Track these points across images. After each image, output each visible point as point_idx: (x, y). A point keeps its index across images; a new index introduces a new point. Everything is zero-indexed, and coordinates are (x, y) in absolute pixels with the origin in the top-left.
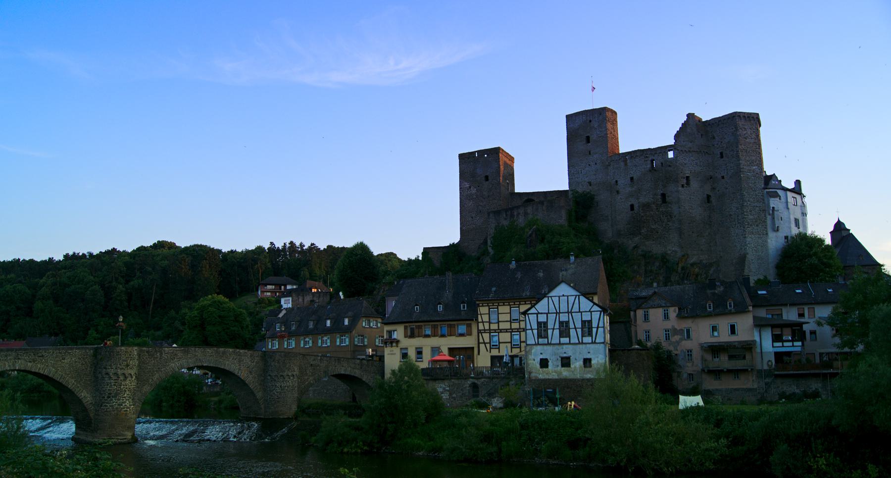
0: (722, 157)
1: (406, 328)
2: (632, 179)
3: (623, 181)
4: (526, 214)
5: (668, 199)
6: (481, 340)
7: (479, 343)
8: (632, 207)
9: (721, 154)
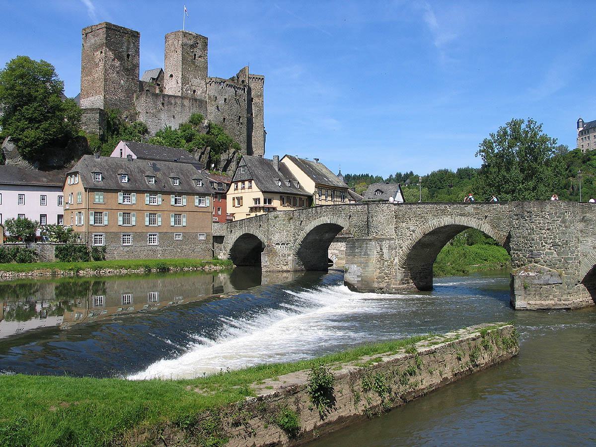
1: (281, 197)
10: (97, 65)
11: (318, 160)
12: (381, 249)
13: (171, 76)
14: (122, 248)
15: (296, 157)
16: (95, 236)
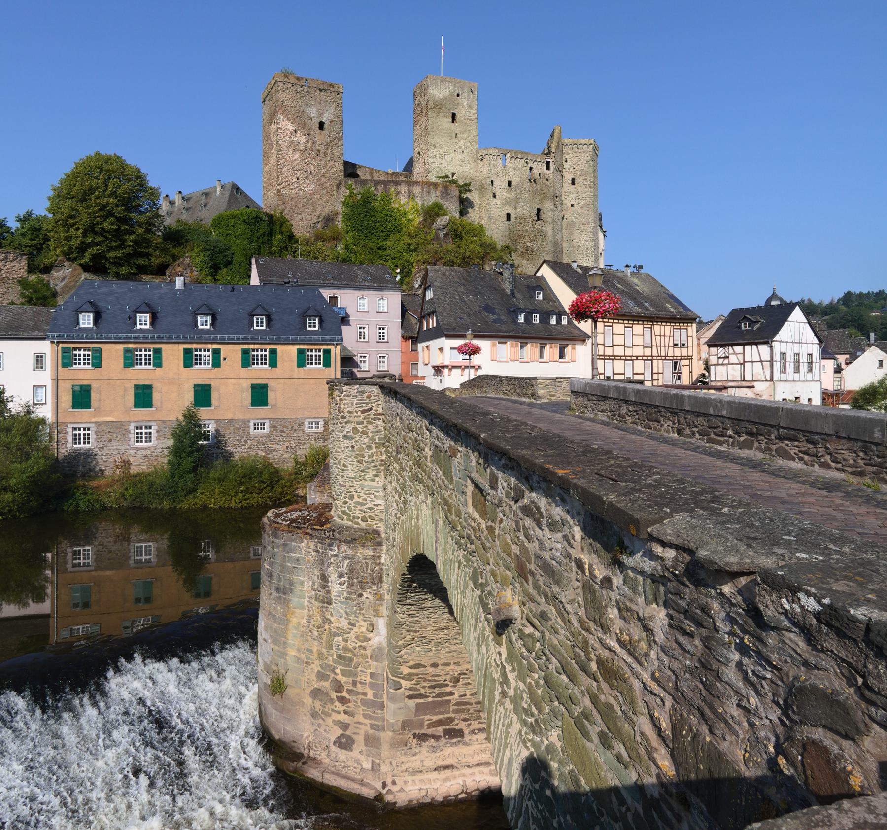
2: (509, 183)
3: (500, 185)
4: (410, 194)
5: (542, 216)
8: (508, 216)
9: (573, 180)
10: (272, 145)
11: (641, 267)
12: (324, 578)
13: (419, 153)
14: (132, 452)
15: (574, 266)
16: (75, 429)
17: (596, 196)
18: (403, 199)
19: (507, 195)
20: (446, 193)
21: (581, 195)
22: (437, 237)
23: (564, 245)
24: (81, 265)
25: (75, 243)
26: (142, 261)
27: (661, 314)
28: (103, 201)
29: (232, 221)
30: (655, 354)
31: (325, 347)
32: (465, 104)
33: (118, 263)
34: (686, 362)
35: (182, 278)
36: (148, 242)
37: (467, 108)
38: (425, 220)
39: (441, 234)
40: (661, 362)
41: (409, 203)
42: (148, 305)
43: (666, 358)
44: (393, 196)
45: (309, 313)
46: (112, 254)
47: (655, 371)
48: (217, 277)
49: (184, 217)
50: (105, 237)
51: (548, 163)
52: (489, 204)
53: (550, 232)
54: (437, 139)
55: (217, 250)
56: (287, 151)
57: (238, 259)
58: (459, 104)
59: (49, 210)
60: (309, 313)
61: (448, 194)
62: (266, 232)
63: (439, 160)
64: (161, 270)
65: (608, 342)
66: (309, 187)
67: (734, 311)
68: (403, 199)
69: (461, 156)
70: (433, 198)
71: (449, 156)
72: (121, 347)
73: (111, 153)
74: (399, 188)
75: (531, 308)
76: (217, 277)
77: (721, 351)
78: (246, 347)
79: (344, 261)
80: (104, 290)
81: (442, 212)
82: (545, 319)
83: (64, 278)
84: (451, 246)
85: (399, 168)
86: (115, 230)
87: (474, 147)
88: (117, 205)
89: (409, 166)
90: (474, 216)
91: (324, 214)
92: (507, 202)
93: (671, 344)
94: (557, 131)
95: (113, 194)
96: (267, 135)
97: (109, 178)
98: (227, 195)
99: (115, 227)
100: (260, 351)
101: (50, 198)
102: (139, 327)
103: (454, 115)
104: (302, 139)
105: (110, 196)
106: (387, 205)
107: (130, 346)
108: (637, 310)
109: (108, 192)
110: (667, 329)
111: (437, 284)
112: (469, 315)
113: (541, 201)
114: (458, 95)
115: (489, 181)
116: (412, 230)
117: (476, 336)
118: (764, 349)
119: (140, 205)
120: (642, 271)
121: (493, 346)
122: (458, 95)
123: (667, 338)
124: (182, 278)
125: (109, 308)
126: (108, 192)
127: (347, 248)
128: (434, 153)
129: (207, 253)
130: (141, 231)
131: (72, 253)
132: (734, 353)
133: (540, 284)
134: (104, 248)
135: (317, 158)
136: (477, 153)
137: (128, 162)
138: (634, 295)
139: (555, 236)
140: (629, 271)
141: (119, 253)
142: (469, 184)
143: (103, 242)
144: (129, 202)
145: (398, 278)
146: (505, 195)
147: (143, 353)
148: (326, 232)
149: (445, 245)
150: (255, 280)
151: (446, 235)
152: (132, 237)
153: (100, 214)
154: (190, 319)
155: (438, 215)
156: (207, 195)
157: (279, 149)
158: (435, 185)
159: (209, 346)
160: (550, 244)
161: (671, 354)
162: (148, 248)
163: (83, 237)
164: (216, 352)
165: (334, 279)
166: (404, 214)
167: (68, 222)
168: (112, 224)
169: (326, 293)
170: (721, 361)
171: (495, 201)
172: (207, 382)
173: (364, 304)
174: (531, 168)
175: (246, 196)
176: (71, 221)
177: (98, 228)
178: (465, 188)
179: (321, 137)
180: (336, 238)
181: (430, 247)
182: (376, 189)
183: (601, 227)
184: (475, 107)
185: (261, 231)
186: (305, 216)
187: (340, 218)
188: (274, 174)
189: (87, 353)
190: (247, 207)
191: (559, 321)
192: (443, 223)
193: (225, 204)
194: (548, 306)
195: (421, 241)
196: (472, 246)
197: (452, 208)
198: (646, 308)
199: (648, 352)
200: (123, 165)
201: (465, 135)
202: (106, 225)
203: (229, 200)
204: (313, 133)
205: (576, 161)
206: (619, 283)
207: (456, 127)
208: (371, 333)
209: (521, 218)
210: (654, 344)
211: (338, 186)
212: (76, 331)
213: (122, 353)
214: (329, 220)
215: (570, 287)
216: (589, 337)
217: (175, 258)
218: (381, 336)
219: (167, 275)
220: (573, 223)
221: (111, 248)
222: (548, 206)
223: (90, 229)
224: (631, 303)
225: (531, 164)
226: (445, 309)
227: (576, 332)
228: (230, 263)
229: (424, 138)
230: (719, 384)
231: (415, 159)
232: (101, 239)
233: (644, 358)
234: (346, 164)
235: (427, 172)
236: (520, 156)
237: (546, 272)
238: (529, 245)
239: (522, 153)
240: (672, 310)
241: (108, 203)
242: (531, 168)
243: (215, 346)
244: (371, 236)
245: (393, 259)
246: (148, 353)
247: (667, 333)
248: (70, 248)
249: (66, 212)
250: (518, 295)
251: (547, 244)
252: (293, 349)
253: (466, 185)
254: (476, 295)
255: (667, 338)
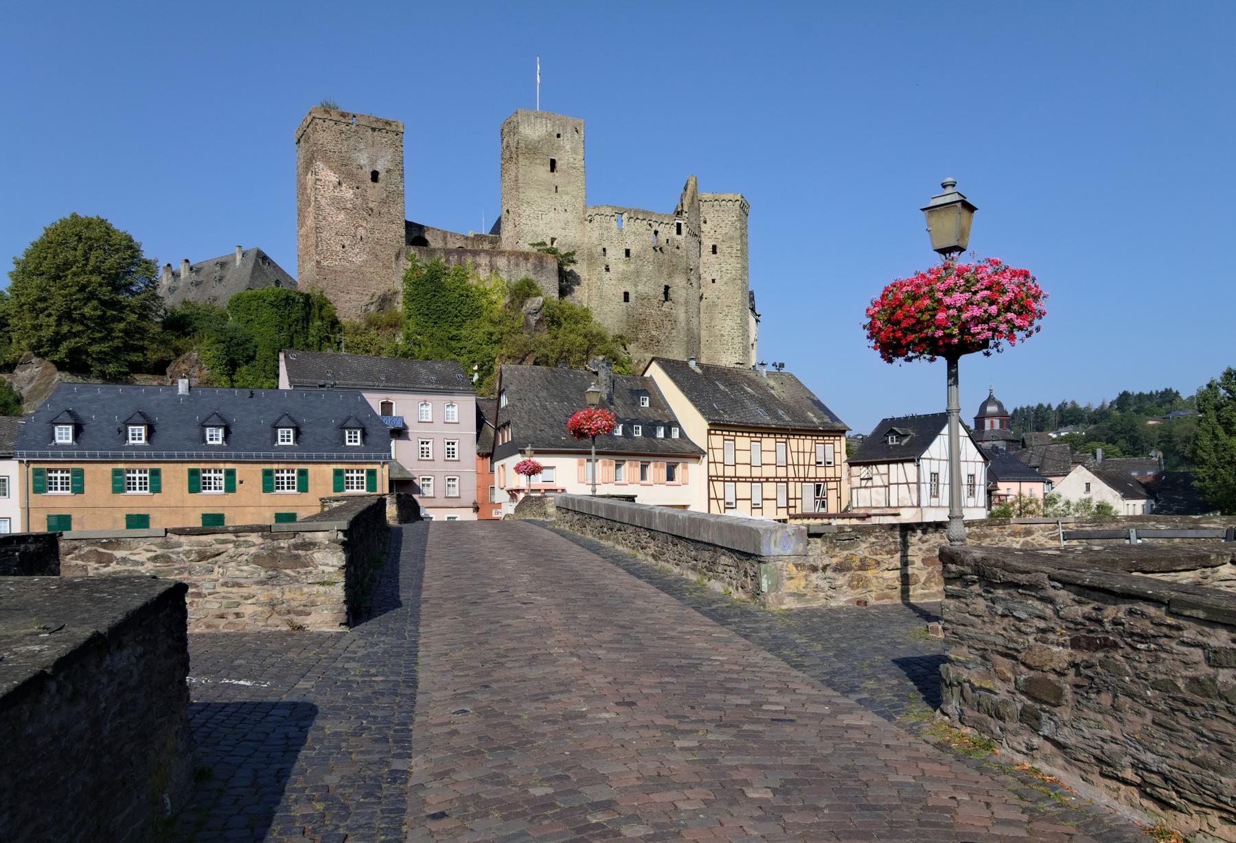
0: (714, 251)
2: (628, 252)
3: (615, 255)
4: (493, 268)
5: (671, 295)
6: (712, 496)
7: (709, 499)
8: (626, 295)
9: (714, 247)
11: (782, 365)
15: (692, 364)
17: (745, 268)
18: (483, 274)
19: (625, 267)
20: (540, 265)
21: (725, 267)
22: (527, 324)
23: (703, 333)
24: (53, 362)
25: (47, 333)
26: (135, 357)
27: (798, 425)
28: (83, 279)
29: (255, 303)
30: (791, 474)
31: (370, 467)
32: (568, 147)
33: (103, 359)
34: (832, 485)
35: (186, 381)
36: (142, 332)
37: (570, 153)
38: (512, 302)
39: (533, 320)
40: (799, 485)
41: (490, 280)
42: (142, 414)
43: (805, 480)
44: (470, 269)
45: (349, 424)
46: (95, 348)
47: (791, 495)
48: (235, 377)
49: (190, 297)
50: (86, 325)
51: (679, 225)
52: (600, 279)
53: (682, 316)
54: (531, 194)
55: (235, 341)
56: (328, 209)
57: (262, 353)
58: (559, 148)
59: (12, 290)
60: (349, 424)
61: (542, 267)
62: (302, 318)
63: (534, 221)
64: (160, 368)
65: (729, 460)
66: (358, 257)
67: (885, 420)
68: (483, 274)
69: (563, 216)
70: (524, 272)
71: (546, 216)
72: (109, 468)
73: (92, 214)
74: (478, 259)
75: (633, 417)
76: (235, 377)
77: (863, 471)
78: (268, 467)
79: (405, 355)
80: (86, 396)
81: (534, 292)
82: (650, 429)
83: (32, 379)
84: (545, 336)
85: (485, 230)
86: (99, 317)
87: (580, 205)
88: (101, 285)
89: (497, 229)
90: (581, 296)
91: (379, 293)
92: (624, 277)
93: (813, 462)
94: (692, 183)
95: (97, 270)
96: (302, 187)
97: (90, 249)
98: (250, 265)
99: (99, 313)
100: (286, 473)
101: (11, 274)
102: (131, 442)
103: (553, 163)
104: (349, 194)
105: (91, 273)
106: (462, 282)
107: (120, 466)
108: (767, 419)
109: (89, 268)
110: (807, 443)
111: (512, 388)
112: (551, 426)
113: (670, 276)
114: (558, 136)
115: (600, 249)
116: (496, 316)
117: (537, 453)
118: (911, 468)
119: (131, 284)
120: (783, 370)
121: (581, 464)
122: (558, 136)
123: (807, 455)
124: (186, 381)
125: (92, 419)
126: (89, 268)
127: (408, 337)
128: (528, 212)
129: (222, 346)
130: (133, 317)
131: (42, 346)
132: (878, 474)
133: (648, 389)
134: (85, 340)
135: (369, 218)
136: (585, 212)
137: (115, 226)
138: (767, 401)
139: (688, 322)
140: (764, 370)
141: (104, 347)
142: (574, 253)
143: (83, 332)
144: (117, 282)
145: (476, 377)
146: (622, 267)
147: (137, 475)
148: (382, 317)
149: (538, 334)
150: (284, 383)
151: (539, 322)
152: (122, 326)
153: (78, 296)
154: (197, 431)
155: (528, 296)
156: (223, 265)
157: (318, 208)
158: (526, 256)
159: (221, 466)
160: (682, 332)
161: (812, 474)
162: (142, 339)
163: (57, 326)
164: (230, 474)
165: (388, 379)
166: (485, 294)
167: (37, 307)
168: (95, 309)
169: (374, 400)
170: (864, 483)
171: (608, 275)
172: (219, 511)
173: (427, 412)
174: (656, 233)
175: (276, 266)
176: (40, 305)
177: (76, 314)
178: (569, 258)
179: (374, 192)
180: (394, 325)
181: (517, 337)
182: (447, 261)
183: (753, 310)
184: (581, 151)
185: (294, 316)
186: (354, 296)
187: (400, 298)
188: (312, 240)
189: (65, 475)
190: (277, 283)
191: (668, 434)
192: (535, 305)
193: (247, 279)
194: (655, 415)
195: (506, 329)
196: (572, 336)
197: (549, 286)
198: (779, 418)
199: (781, 472)
200: (109, 231)
201: (569, 189)
202: (87, 310)
203: (253, 272)
204: (363, 186)
205: (718, 223)
206: (749, 386)
207: (557, 178)
208: (437, 449)
209: (642, 298)
210: (790, 462)
211: (398, 256)
212: (52, 449)
213: (110, 475)
214: (385, 301)
215: (683, 391)
216: (704, 453)
217: (178, 352)
218: (450, 453)
219: (169, 374)
220: (714, 305)
221: (94, 340)
222: (678, 283)
223: (66, 316)
224: (761, 411)
225: (655, 227)
226: (521, 418)
227: (688, 448)
228: (252, 358)
229: (514, 193)
230: (862, 512)
231: (503, 219)
232: (81, 328)
233: (776, 480)
234: (409, 226)
235: (518, 237)
236: (640, 217)
237: (656, 373)
238: (654, 333)
239: (644, 212)
240: (815, 420)
241: (89, 282)
242: (656, 233)
243: (229, 466)
244: (441, 323)
245: (470, 352)
246: (143, 475)
247: (808, 449)
248: (40, 340)
249: (35, 293)
250: (617, 401)
251: (678, 332)
252: (329, 469)
253: (568, 254)
254: (562, 401)
255: (807, 455)
